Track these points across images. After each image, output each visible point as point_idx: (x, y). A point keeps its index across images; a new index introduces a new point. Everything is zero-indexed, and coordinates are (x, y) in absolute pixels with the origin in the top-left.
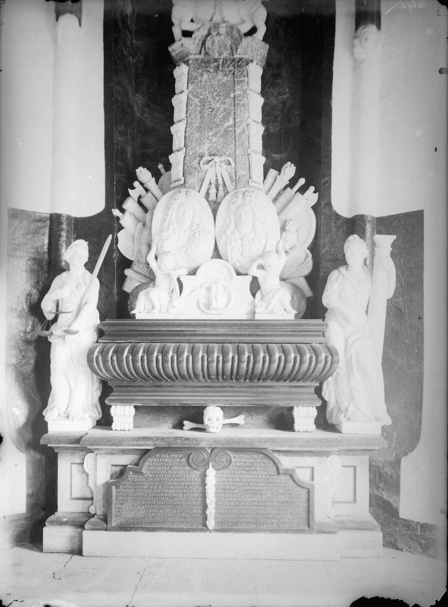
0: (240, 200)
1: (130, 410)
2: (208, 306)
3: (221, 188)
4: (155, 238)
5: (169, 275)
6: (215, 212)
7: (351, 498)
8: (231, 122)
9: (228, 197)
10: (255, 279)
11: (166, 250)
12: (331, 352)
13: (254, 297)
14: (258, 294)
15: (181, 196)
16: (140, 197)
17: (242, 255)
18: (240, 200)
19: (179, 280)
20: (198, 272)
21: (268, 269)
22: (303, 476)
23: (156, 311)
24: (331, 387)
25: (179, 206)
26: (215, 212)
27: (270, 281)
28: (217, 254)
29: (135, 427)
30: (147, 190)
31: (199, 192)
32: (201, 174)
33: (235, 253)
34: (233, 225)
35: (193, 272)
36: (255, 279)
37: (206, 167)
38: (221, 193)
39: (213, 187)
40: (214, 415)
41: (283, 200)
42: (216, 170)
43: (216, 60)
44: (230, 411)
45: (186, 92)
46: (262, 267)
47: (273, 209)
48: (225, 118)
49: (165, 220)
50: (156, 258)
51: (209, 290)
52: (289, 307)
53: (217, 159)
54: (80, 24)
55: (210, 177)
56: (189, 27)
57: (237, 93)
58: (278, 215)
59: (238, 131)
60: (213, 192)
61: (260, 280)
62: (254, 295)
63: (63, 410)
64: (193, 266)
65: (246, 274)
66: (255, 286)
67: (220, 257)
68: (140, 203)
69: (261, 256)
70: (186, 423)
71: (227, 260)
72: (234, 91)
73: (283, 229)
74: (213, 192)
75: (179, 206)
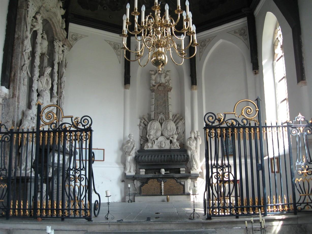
0: (167, 123)
1: (144, 170)
2: (161, 147)
3: (163, 120)
5: (151, 140)
6: (161, 125)
8: (164, 105)
9: (164, 122)
10: (171, 140)
11: (151, 134)
12: (188, 156)
14: (172, 144)
15: (154, 123)
16: (144, 122)
17: (168, 135)
18: (167, 123)
19: (154, 140)
20: (159, 139)
21: (174, 138)
24: (189, 164)
25: (153, 124)
26: (161, 125)
28: (162, 135)
29: (145, 174)
30: (145, 120)
31: (157, 120)
32: (158, 117)
33: (166, 134)
34: (165, 129)
35: (157, 139)
37: (159, 115)
38: (163, 121)
39: (161, 119)
40: (163, 171)
41: (177, 122)
42: (161, 116)
45: (154, 98)
46: (172, 138)
48: (163, 104)
49: (150, 127)
50: (148, 136)
51: (161, 143)
52: (179, 146)
53: (162, 113)
54: (127, 81)
55: (160, 117)
56: (154, 84)
57: (166, 98)
60: (161, 121)
61: (172, 140)
62: (171, 144)
66: (171, 142)
67: (163, 135)
69: (173, 135)
70: (157, 173)
71: (164, 136)
72: (165, 98)
73: (177, 128)
74: (161, 121)
75: (153, 124)
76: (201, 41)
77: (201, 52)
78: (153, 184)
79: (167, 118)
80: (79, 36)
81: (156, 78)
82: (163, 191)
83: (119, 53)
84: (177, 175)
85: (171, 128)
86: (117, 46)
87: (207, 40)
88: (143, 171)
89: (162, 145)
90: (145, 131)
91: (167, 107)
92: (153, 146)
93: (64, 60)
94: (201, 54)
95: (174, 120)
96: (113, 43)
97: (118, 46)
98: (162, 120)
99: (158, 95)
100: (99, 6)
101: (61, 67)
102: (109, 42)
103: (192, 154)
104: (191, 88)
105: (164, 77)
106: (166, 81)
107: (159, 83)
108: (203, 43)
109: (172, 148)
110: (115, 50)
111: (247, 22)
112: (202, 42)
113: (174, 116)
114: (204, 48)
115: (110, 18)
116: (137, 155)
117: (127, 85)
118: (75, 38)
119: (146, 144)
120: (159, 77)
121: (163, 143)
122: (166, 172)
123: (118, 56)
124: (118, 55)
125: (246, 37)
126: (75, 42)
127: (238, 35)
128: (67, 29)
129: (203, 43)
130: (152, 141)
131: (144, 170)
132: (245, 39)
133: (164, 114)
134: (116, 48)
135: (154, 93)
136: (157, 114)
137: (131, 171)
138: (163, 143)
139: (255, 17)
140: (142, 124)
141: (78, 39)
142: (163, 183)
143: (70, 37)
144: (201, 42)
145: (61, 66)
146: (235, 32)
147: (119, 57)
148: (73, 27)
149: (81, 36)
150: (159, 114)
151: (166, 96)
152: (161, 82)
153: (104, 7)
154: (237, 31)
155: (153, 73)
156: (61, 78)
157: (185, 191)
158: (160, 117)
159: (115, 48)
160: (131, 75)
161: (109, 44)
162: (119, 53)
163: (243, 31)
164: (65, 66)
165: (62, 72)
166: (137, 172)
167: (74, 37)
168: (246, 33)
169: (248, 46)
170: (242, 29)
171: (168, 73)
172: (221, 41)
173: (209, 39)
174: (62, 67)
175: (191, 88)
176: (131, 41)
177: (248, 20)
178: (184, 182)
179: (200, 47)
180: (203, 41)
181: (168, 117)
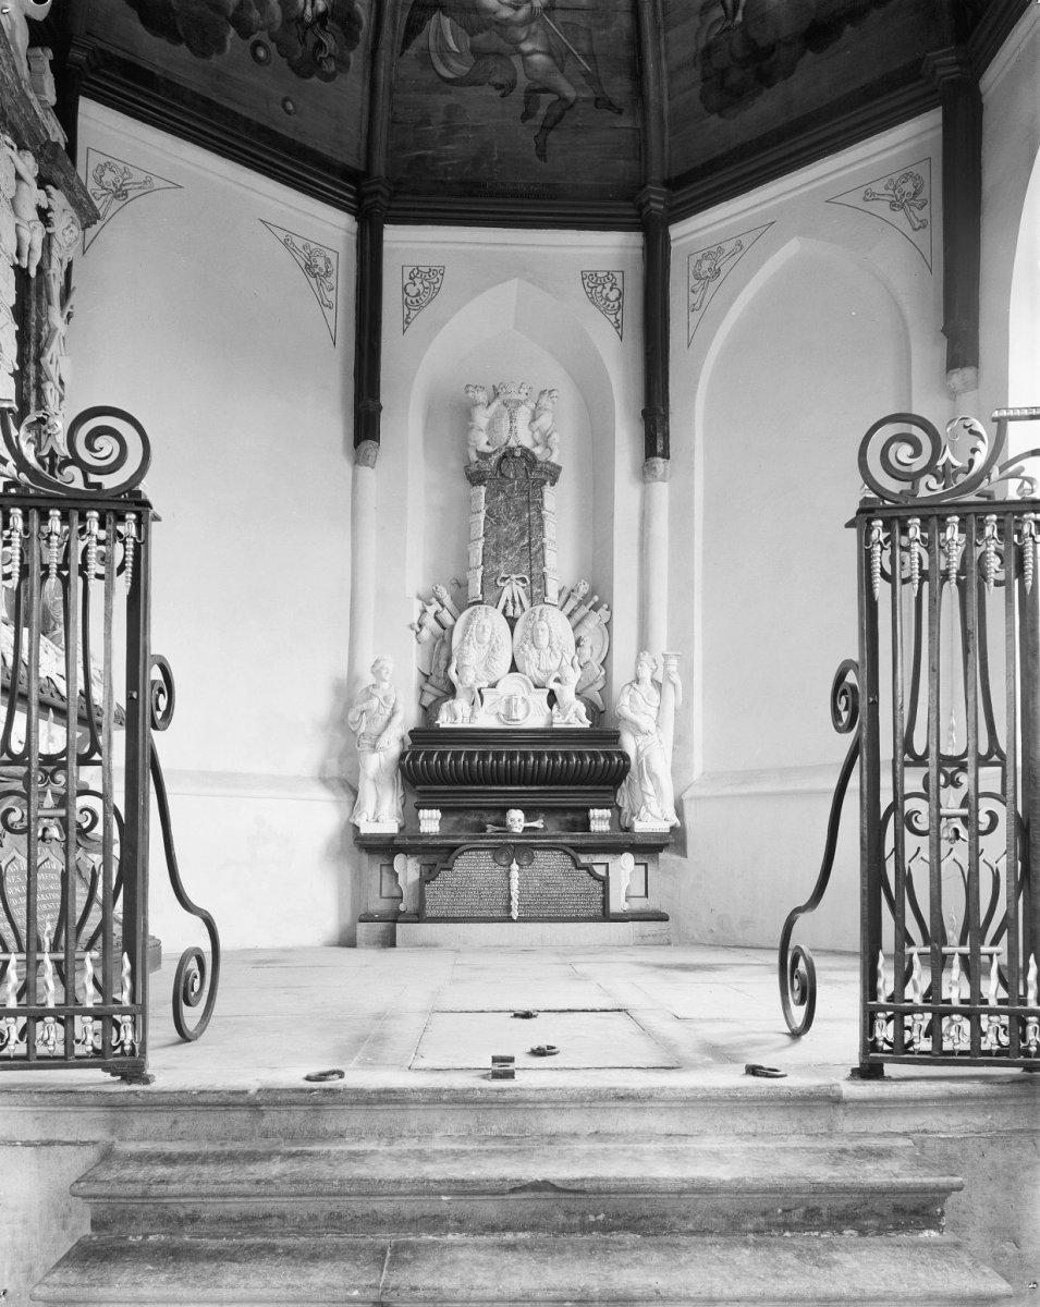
2: (508, 717)
3: (518, 605)
4: (455, 654)
6: (512, 629)
7: (643, 894)
10: (552, 693)
12: (625, 757)
13: (551, 708)
14: (555, 706)
16: (436, 613)
20: (499, 686)
22: (600, 870)
23: (460, 719)
26: (512, 629)
27: (567, 694)
28: (514, 668)
30: (443, 606)
33: (530, 667)
35: (493, 686)
36: (552, 693)
37: (502, 584)
38: (518, 610)
39: (510, 603)
41: (577, 616)
43: (511, 481)
44: (530, 813)
46: (558, 680)
47: (568, 625)
48: (521, 537)
51: (508, 702)
58: (573, 629)
59: (534, 550)
60: (510, 607)
62: (551, 708)
63: (371, 816)
64: (493, 680)
65: (544, 687)
66: (552, 699)
67: (517, 671)
68: (436, 618)
72: (529, 512)
74: (510, 607)
76: (699, 256)
77: (697, 305)
78: (474, 868)
79: (537, 594)
80: (139, 177)
81: (491, 426)
82: (515, 903)
83: (331, 296)
84: (577, 838)
85: (554, 639)
86: (321, 262)
87: (728, 247)
88: (430, 819)
89: (516, 711)
90: (444, 651)
91: (536, 553)
92: (477, 714)
93: (56, 272)
94: (695, 317)
95: (568, 609)
97: (328, 261)
98: (514, 607)
99: (501, 497)
101: (39, 302)
103: (641, 749)
104: (645, 473)
105: (529, 418)
106: (537, 435)
107: (506, 444)
108: (706, 264)
109: (554, 726)
110: (313, 280)
111: (940, 131)
112: (705, 257)
113: (567, 594)
114: (713, 285)
115: (289, 112)
116: (407, 749)
117: (368, 444)
119: (445, 705)
120: (506, 415)
121: (520, 702)
122: (528, 825)
123: (326, 310)
124: (326, 302)
125: (923, 214)
126: (117, 204)
127: (882, 208)
128: (66, 114)
129: (706, 264)
130: (473, 693)
131: (437, 814)
132: (917, 225)
133: (524, 580)
134: (317, 270)
135: (483, 489)
136: (491, 583)
137: (382, 814)
138: (520, 702)
139: (984, 100)
140: (430, 621)
142: (517, 867)
144: (699, 262)
145: (39, 293)
146: (870, 196)
147: (330, 313)
148: (93, 115)
149: (145, 182)
150: (504, 579)
151: (534, 502)
152: (512, 443)
153: (257, 44)
154: (878, 188)
155: (482, 397)
156: (40, 353)
157: (608, 902)
158: (507, 594)
159: (309, 268)
160: (384, 399)
161: (285, 243)
162: (331, 296)
163: (908, 187)
164: (66, 292)
165: (46, 328)
166: (409, 820)
167: (109, 177)
168: (924, 195)
169: (928, 257)
170: (907, 176)
171: (545, 401)
172: (792, 248)
173: (739, 244)
174: (44, 301)
175: (645, 473)
176: (386, 246)
177: (948, 124)
178: (604, 867)
179: (693, 282)
180: (710, 253)
181: (540, 593)
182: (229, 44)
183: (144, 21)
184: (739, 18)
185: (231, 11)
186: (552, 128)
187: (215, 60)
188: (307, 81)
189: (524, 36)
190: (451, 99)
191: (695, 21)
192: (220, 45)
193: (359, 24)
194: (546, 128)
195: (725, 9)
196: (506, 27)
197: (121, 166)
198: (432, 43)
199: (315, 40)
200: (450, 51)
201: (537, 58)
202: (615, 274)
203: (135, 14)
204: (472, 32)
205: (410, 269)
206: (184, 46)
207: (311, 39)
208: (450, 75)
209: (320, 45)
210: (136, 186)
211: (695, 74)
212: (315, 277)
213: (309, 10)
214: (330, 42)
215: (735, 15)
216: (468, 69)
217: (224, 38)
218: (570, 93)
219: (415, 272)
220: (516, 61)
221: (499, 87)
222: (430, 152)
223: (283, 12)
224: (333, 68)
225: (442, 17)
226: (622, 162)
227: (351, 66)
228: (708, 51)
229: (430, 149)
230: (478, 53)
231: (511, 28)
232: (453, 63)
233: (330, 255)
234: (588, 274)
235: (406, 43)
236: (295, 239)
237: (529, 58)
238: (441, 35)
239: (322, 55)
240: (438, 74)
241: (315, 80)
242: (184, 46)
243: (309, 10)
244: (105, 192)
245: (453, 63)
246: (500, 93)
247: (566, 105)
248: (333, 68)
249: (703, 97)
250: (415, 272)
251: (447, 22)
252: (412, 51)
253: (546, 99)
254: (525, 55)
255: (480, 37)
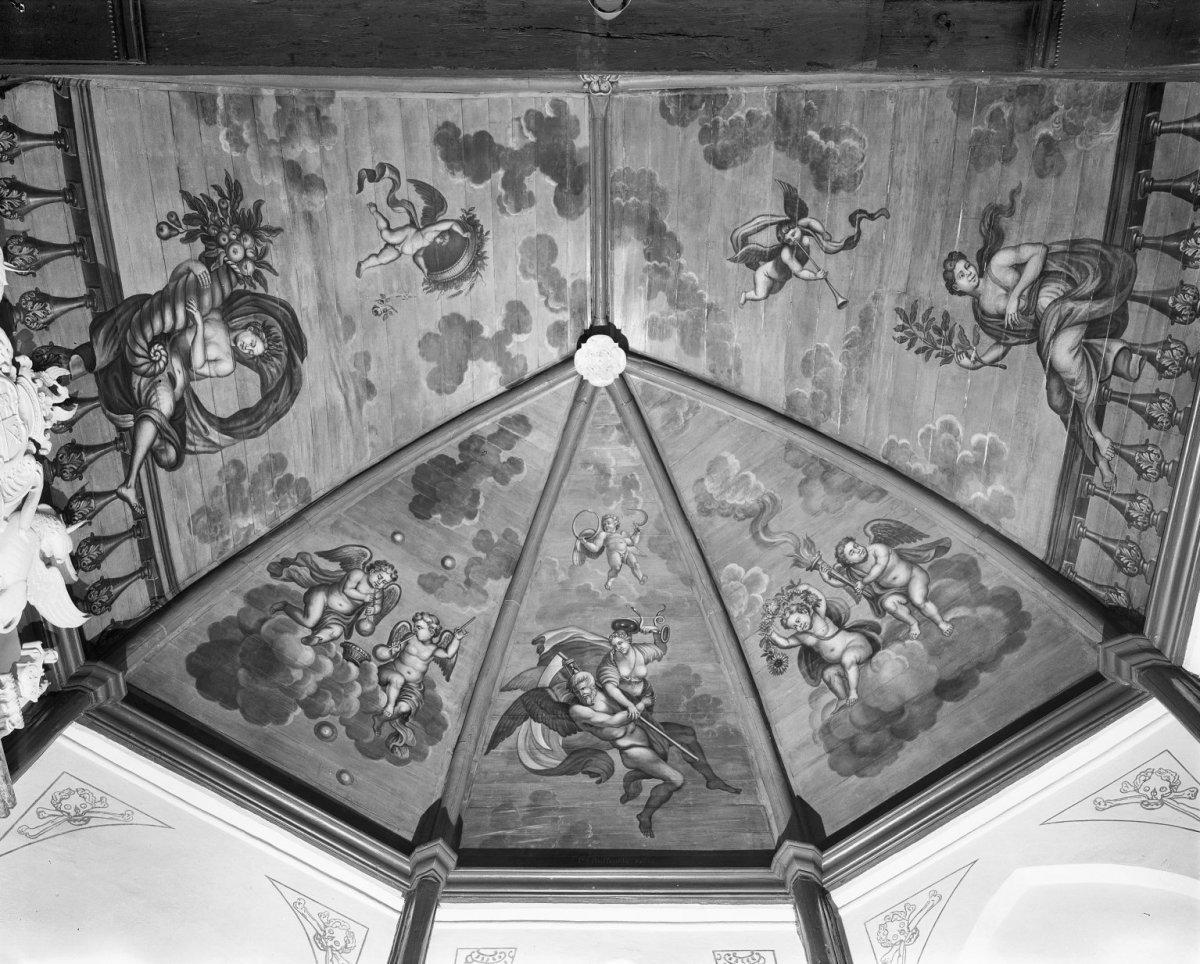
80: (115, 807)
86: (340, 936)
96: (322, 909)
97: (350, 935)
100: (299, 710)
102: (292, 897)
110: (321, 955)
115: (342, 783)
118: (76, 809)
126: (68, 826)
134: (330, 943)
141: (92, 822)
143: (48, 795)
153: (325, 724)
161: (294, 907)
167: (75, 801)
182: (291, 719)
183: (199, 686)
184: (854, 695)
185: (304, 696)
186: (658, 807)
187: (269, 728)
188: (376, 762)
189: (621, 734)
190: (539, 786)
191: (806, 709)
192: (281, 718)
193: (445, 726)
194: (651, 807)
195: (835, 692)
196: (601, 729)
197: (98, 795)
198: (521, 742)
199: (391, 731)
200: (540, 748)
201: (634, 752)
202: (762, 953)
203: (194, 681)
204: (565, 733)
205: (468, 952)
206: (238, 712)
207: (387, 730)
208: (542, 768)
209: (397, 735)
210: (107, 816)
211: (821, 749)
212: (325, 950)
213: (390, 709)
214: (408, 735)
215: (848, 695)
216: (560, 762)
217: (287, 715)
218: (676, 777)
219: (474, 955)
220: (614, 755)
221: (592, 775)
222: (509, 832)
223: (361, 706)
224: (407, 755)
225: (533, 722)
226: (748, 835)
227: (428, 758)
228: (827, 729)
229: (509, 829)
230: (572, 751)
231: (607, 729)
232: (542, 757)
233: (354, 927)
234: (723, 954)
235: (493, 744)
236: (309, 905)
237: (628, 751)
238: (531, 736)
239: (397, 743)
240: (526, 767)
241: (383, 762)
242: (238, 712)
243: (390, 709)
244: (60, 813)
245: (542, 757)
246: (595, 780)
247: (671, 789)
248: (407, 755)
249: (833, 766)
250: (474, 955)
251: (537, 727)
252: (502, 748)
253: (648, 785)
254: (622, 750)
255: (573, 736)
